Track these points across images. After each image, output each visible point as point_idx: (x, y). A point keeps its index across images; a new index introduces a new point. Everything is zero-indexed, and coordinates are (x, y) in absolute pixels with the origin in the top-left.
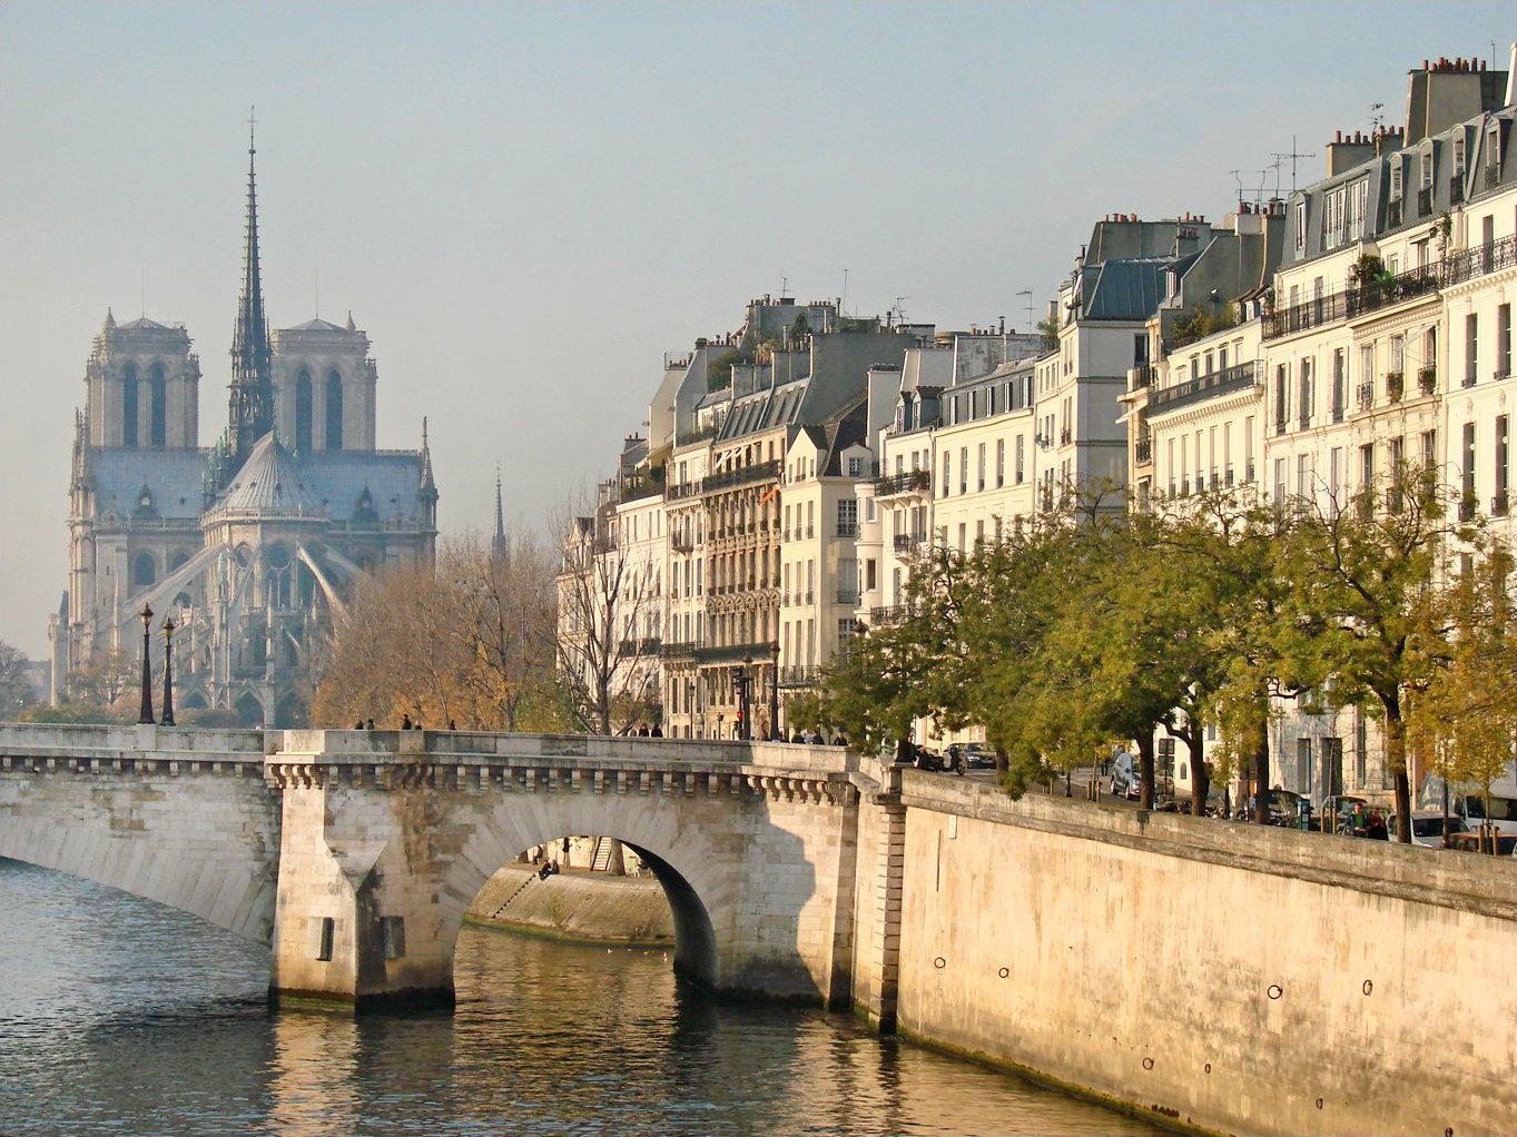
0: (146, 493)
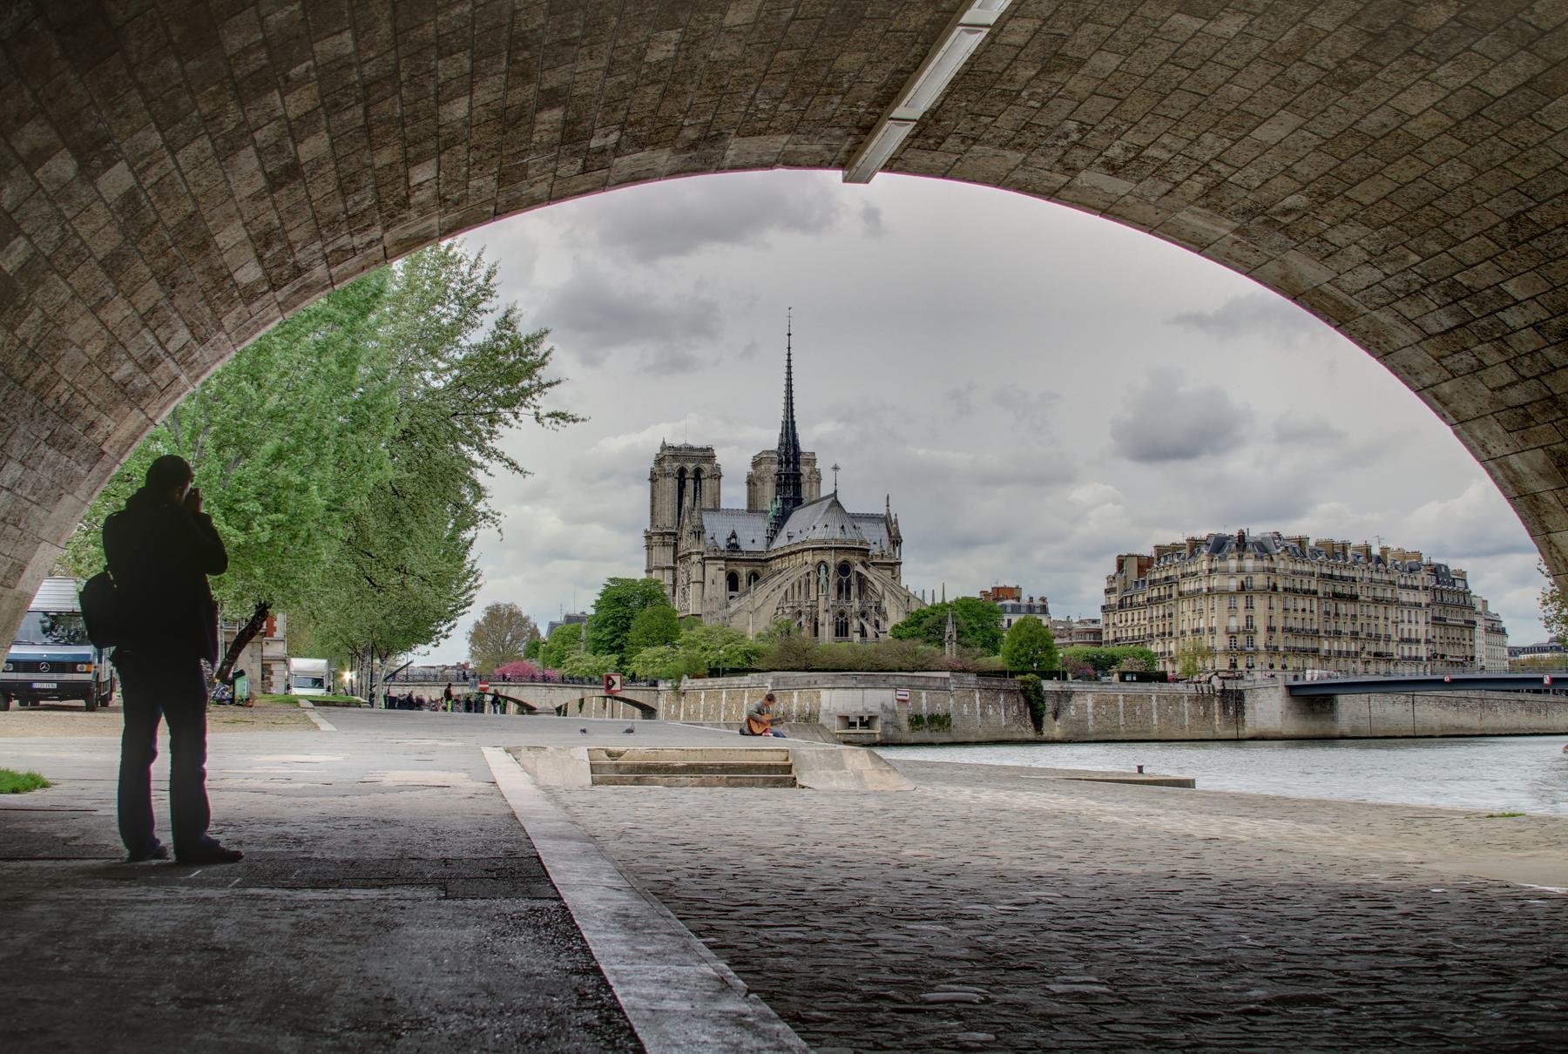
0: (734, 536)
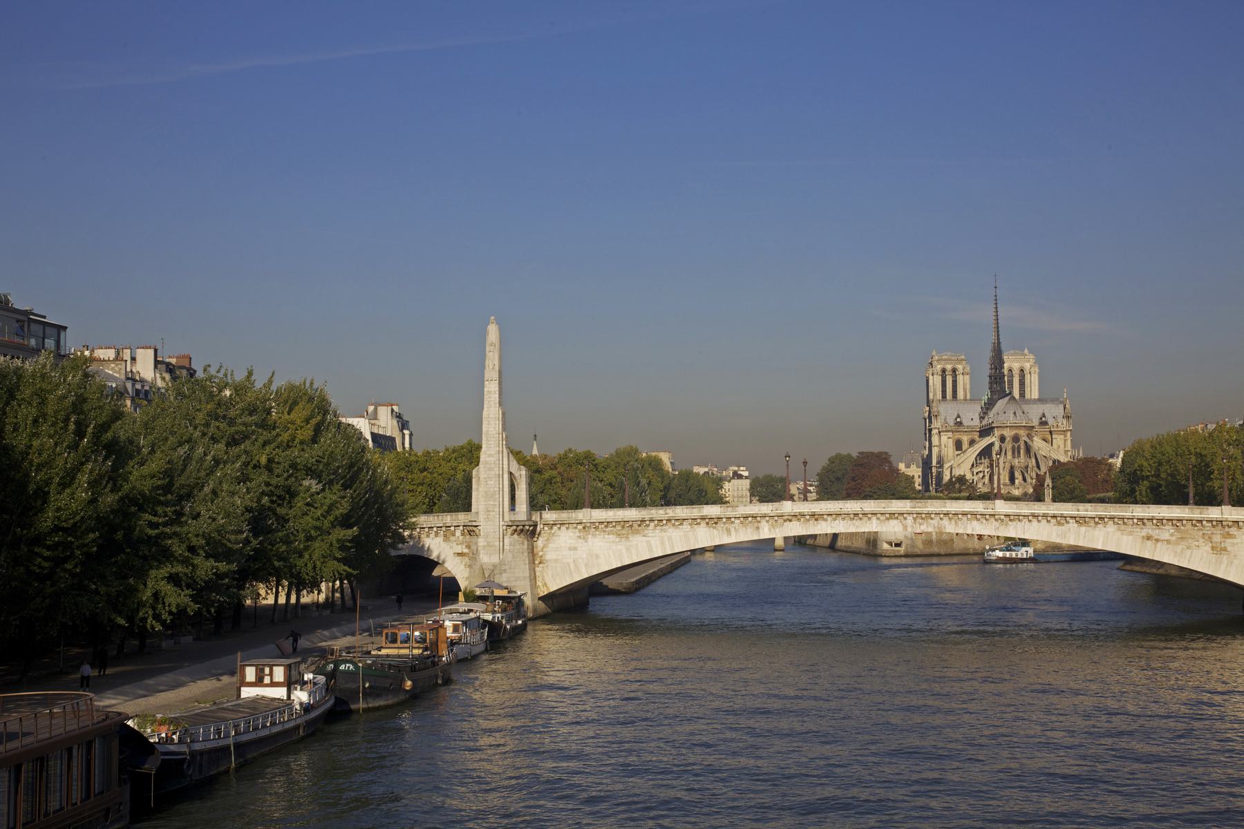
0: (959, 416)
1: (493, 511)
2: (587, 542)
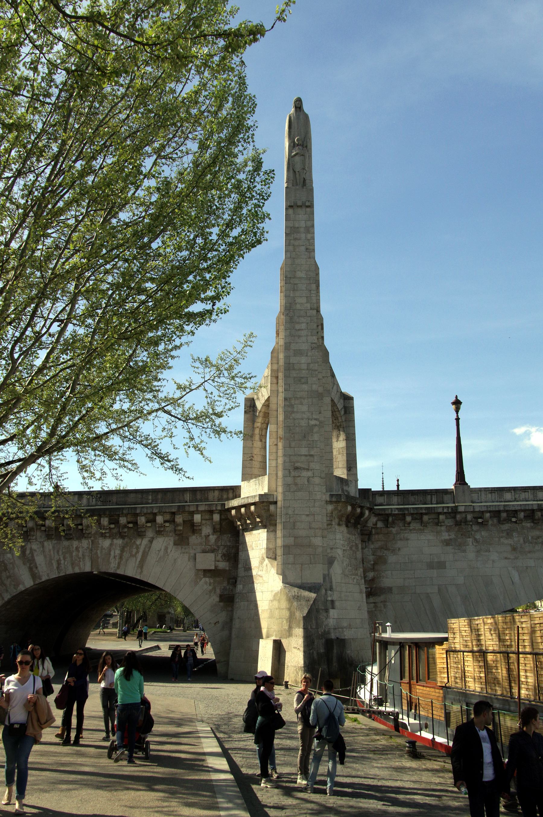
1: (308, 470)
2: (464, 551)
